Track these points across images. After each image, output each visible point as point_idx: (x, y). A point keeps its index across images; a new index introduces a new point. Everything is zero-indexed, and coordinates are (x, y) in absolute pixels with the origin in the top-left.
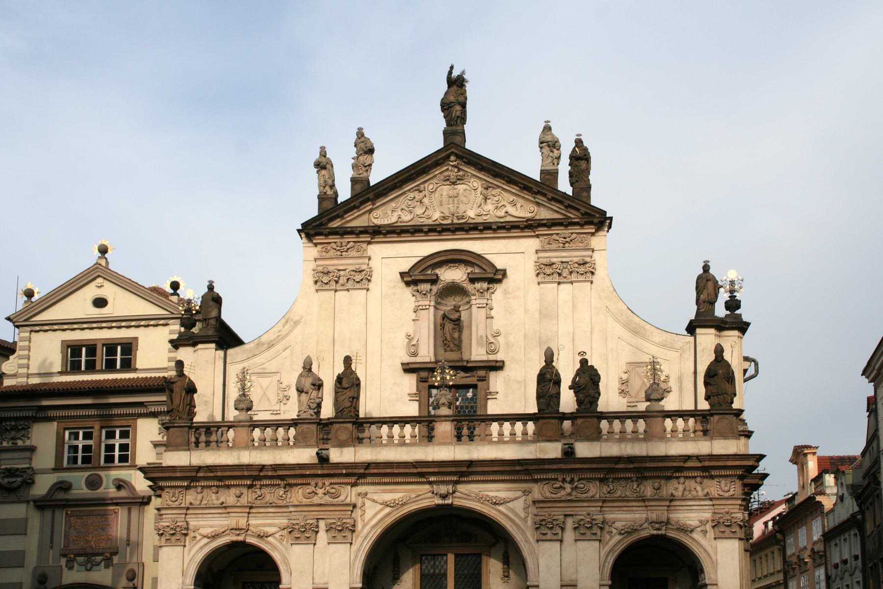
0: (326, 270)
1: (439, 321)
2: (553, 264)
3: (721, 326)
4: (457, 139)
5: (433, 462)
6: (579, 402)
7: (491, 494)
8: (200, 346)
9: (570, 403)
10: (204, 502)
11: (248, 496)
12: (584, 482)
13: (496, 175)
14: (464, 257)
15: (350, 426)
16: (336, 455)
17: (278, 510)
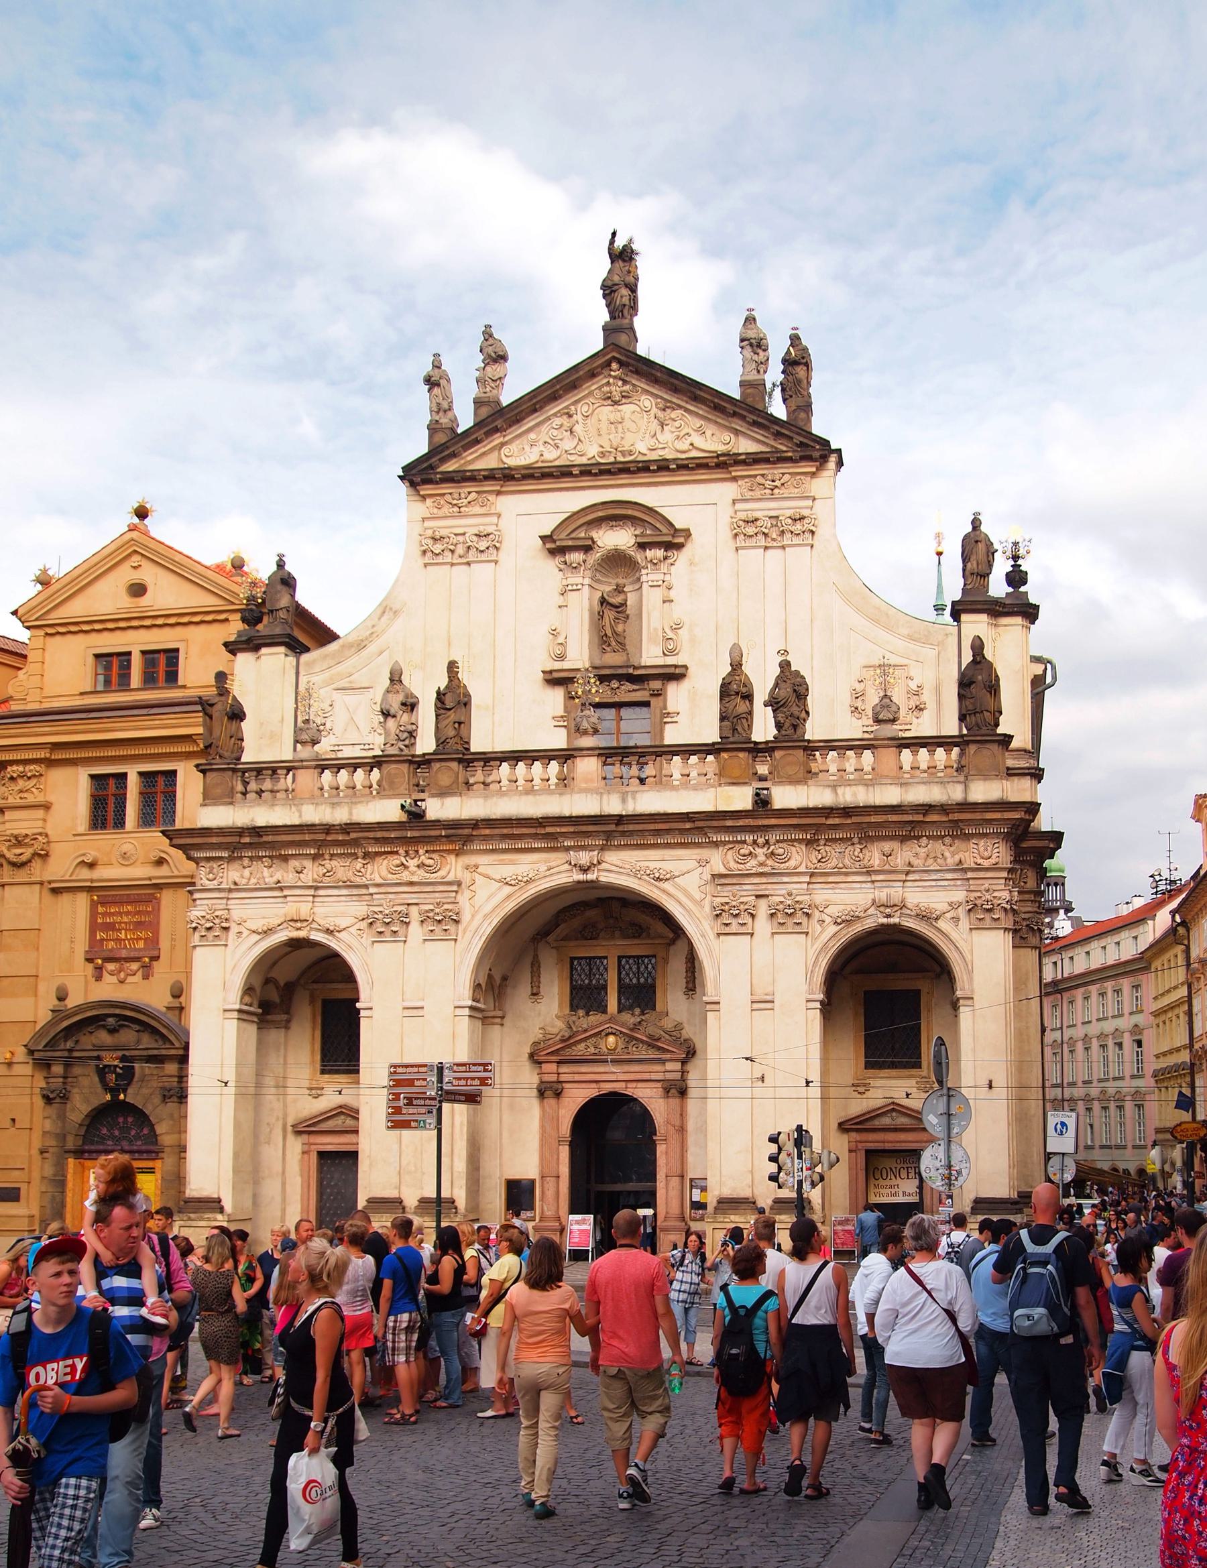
0: (438, 535)
1: (597, 607)
2: (756, 520)
3: (997, 610)
4: (623, 339)
5: (570, 817)
6: (779, 726)
7: (652, 865)
8: (264, 650)
9: (768, 725)
10: (253, 881)
11: (312, 872)
12: (784, 845)
13: (675, 390)
14: (630, 512)
15: (454, 765)
17: (355, 891)
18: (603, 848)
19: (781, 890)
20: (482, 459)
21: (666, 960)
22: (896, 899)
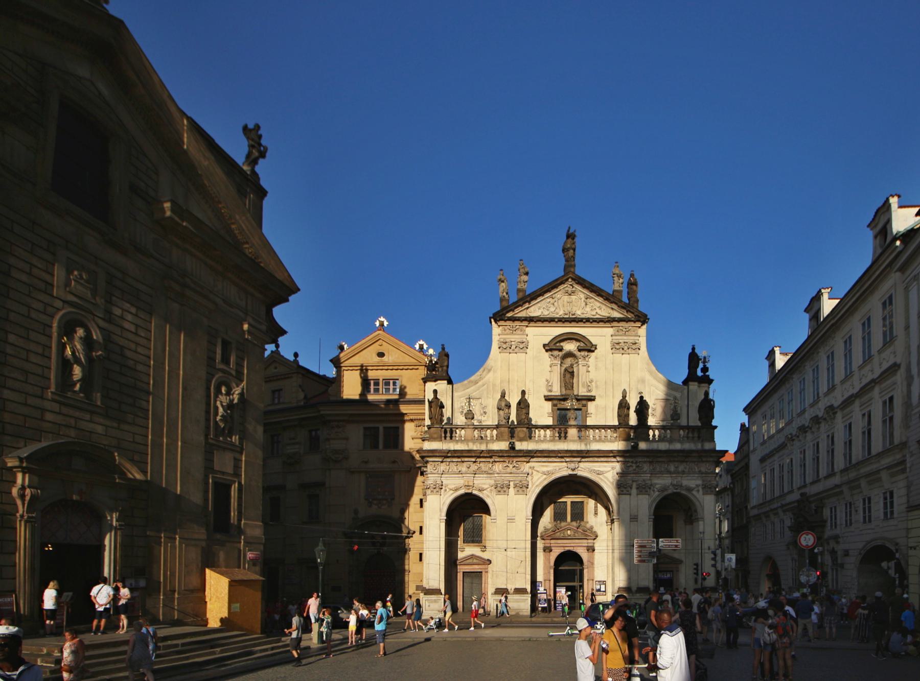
6: (639, 420)
16: (519, 446)
20: (521, 313)
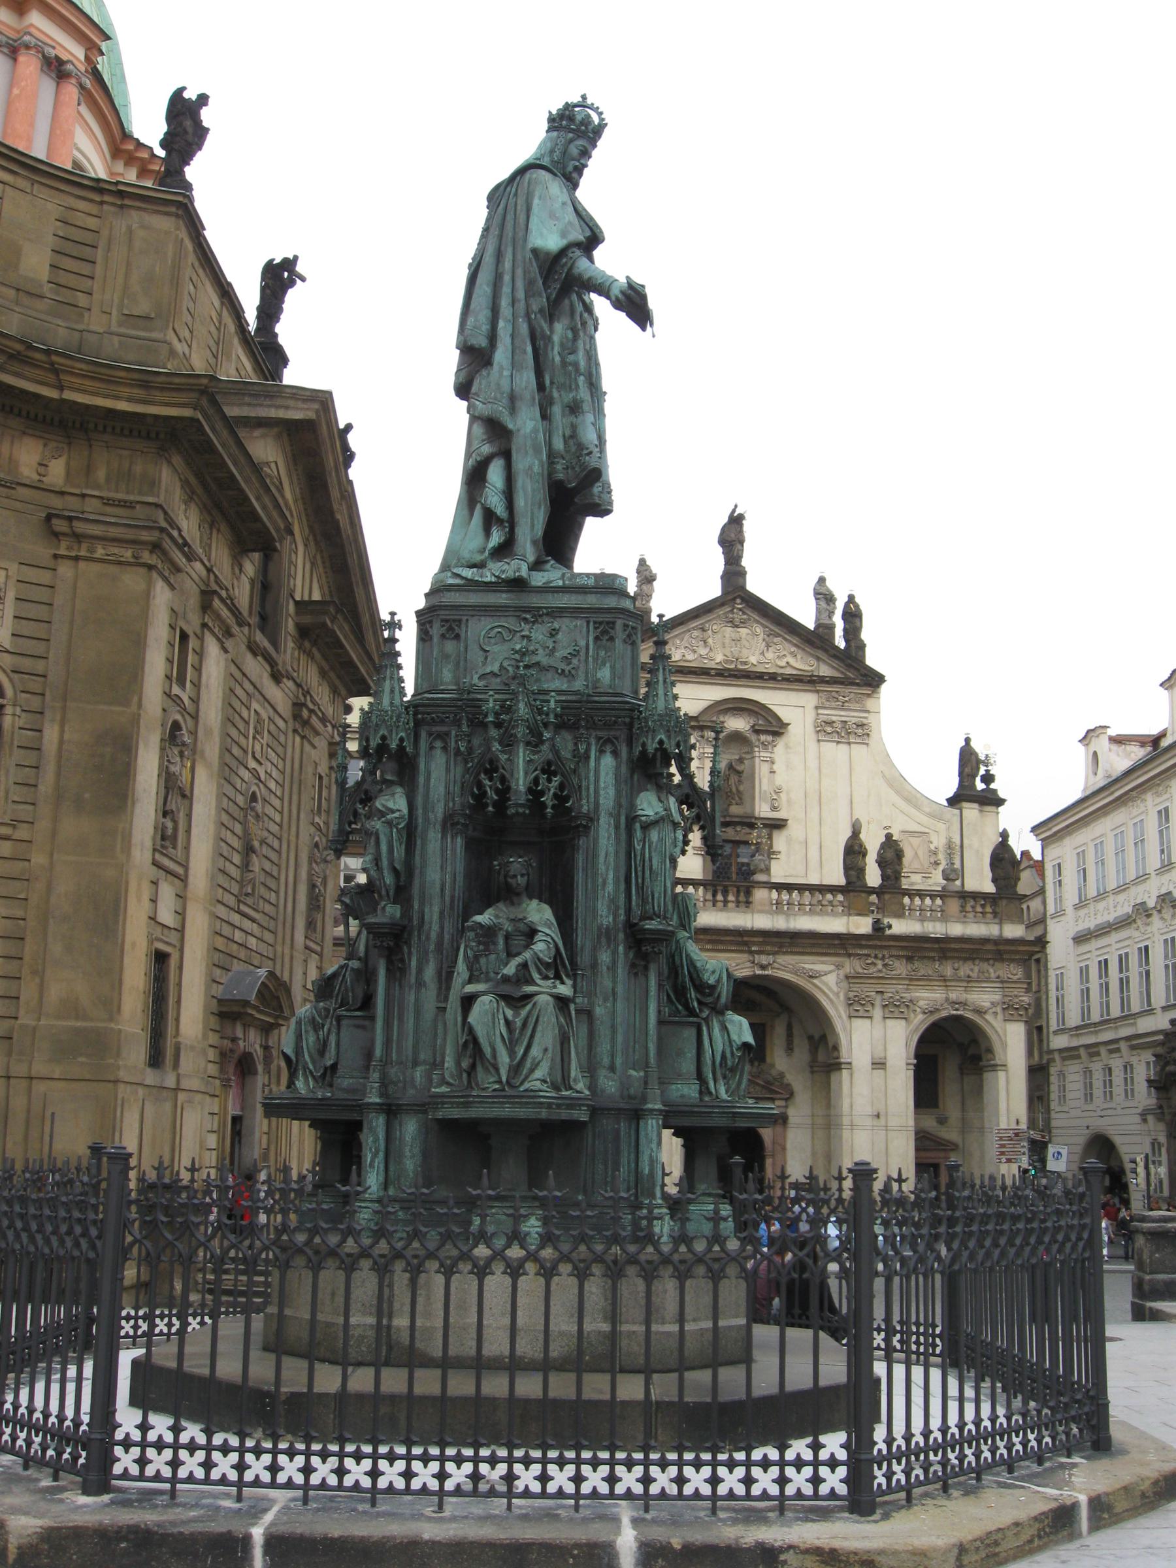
6: (884, 877)
18: (775, 953)
19: (892, 988)
21: (773, 1027)
22: (962, 999)
